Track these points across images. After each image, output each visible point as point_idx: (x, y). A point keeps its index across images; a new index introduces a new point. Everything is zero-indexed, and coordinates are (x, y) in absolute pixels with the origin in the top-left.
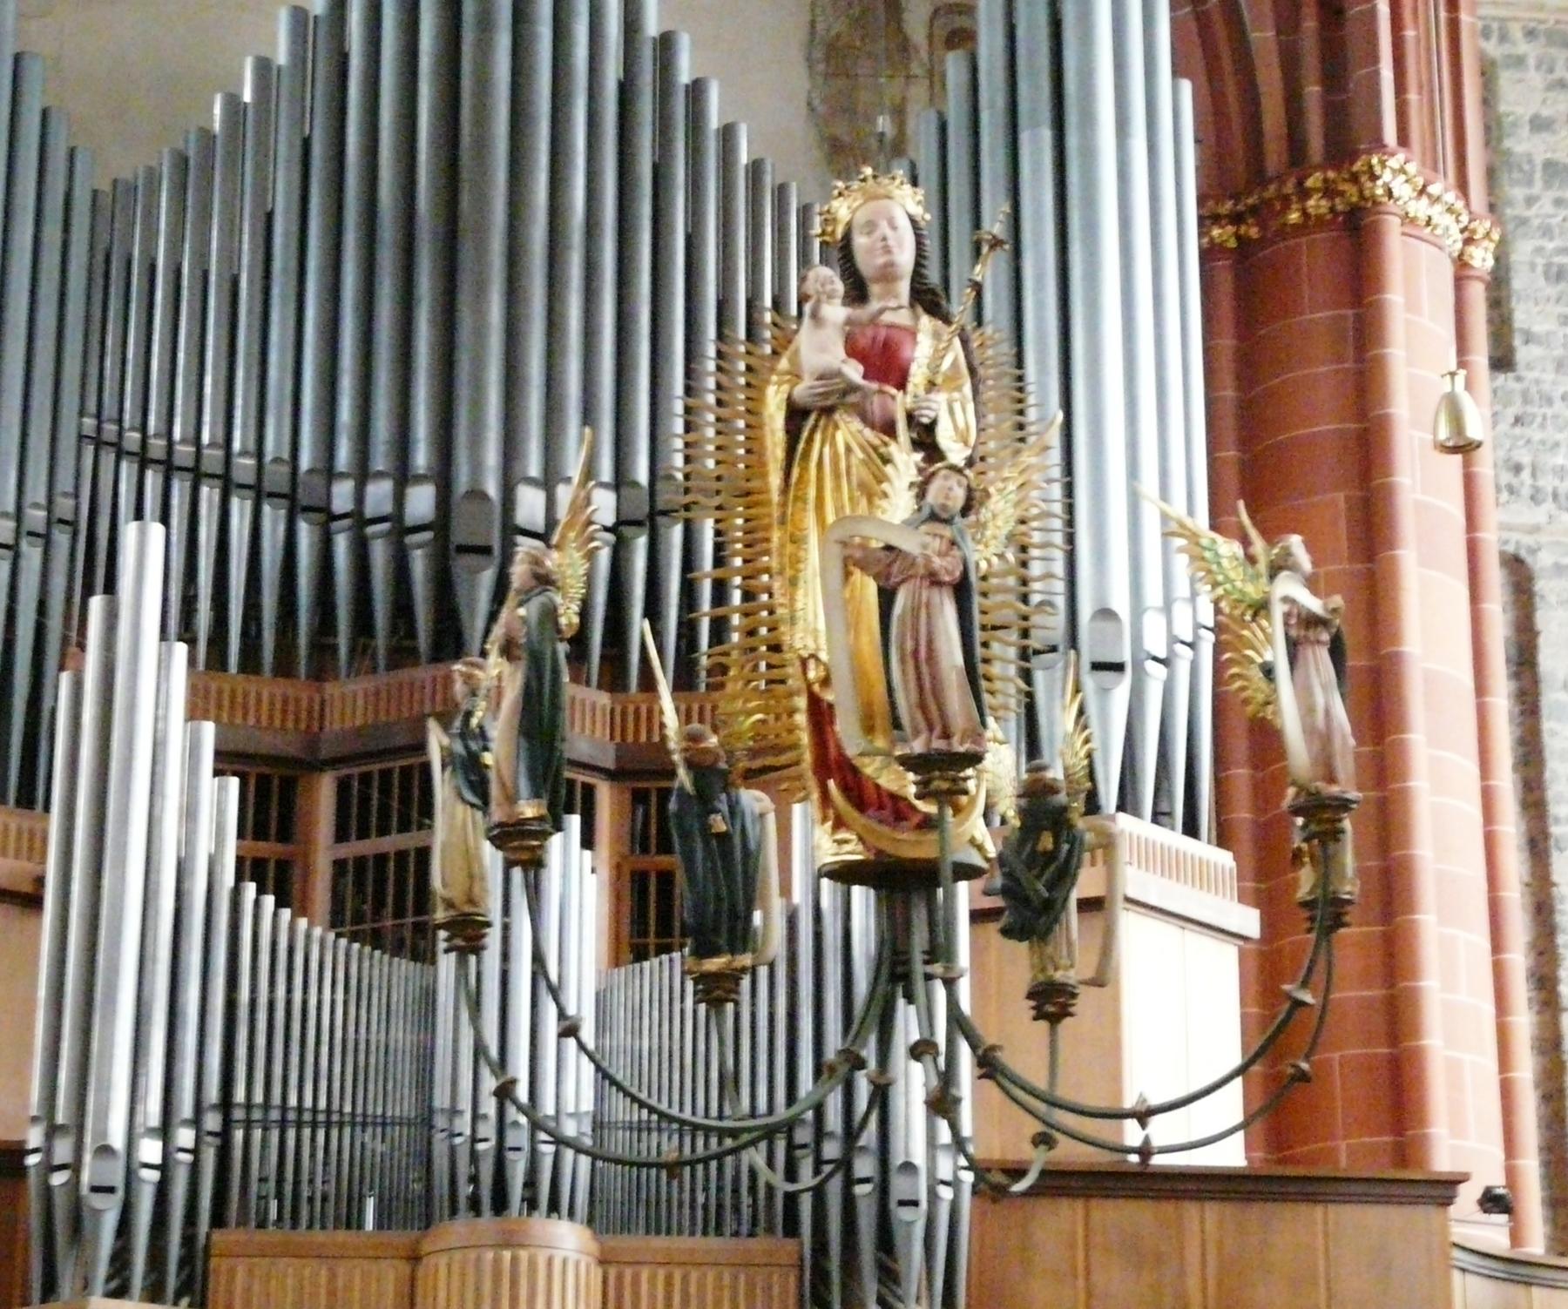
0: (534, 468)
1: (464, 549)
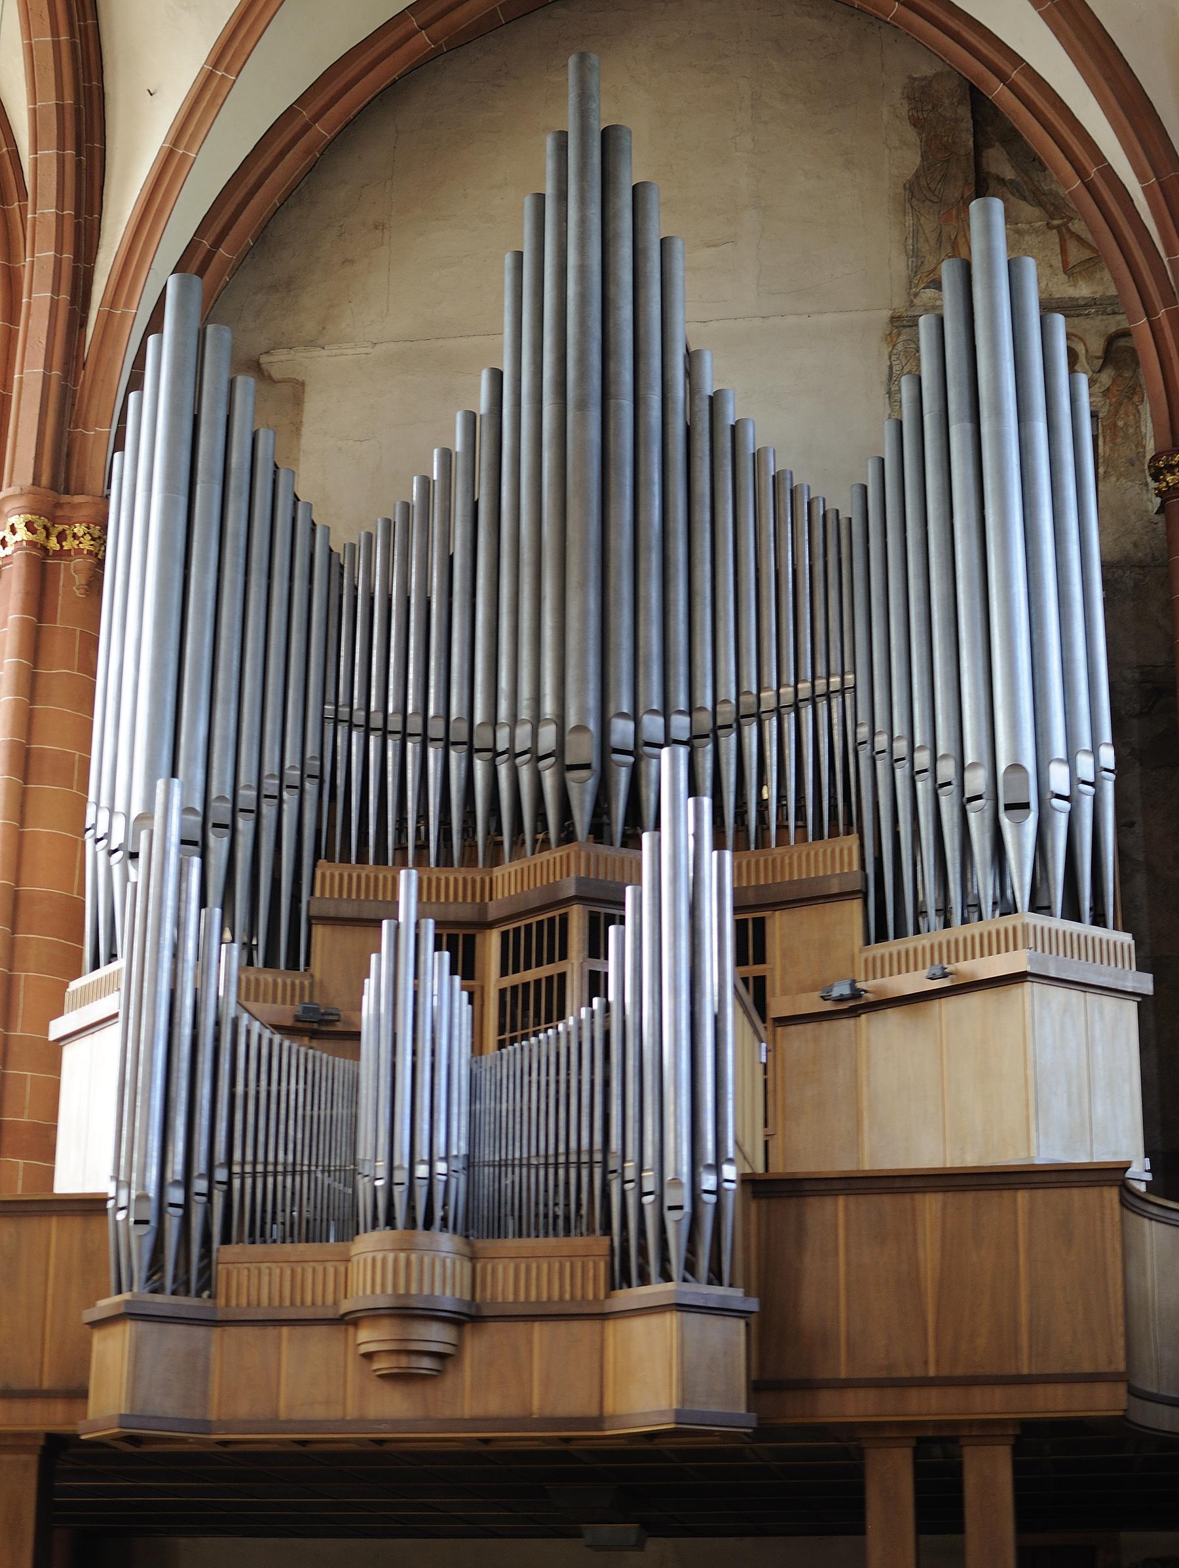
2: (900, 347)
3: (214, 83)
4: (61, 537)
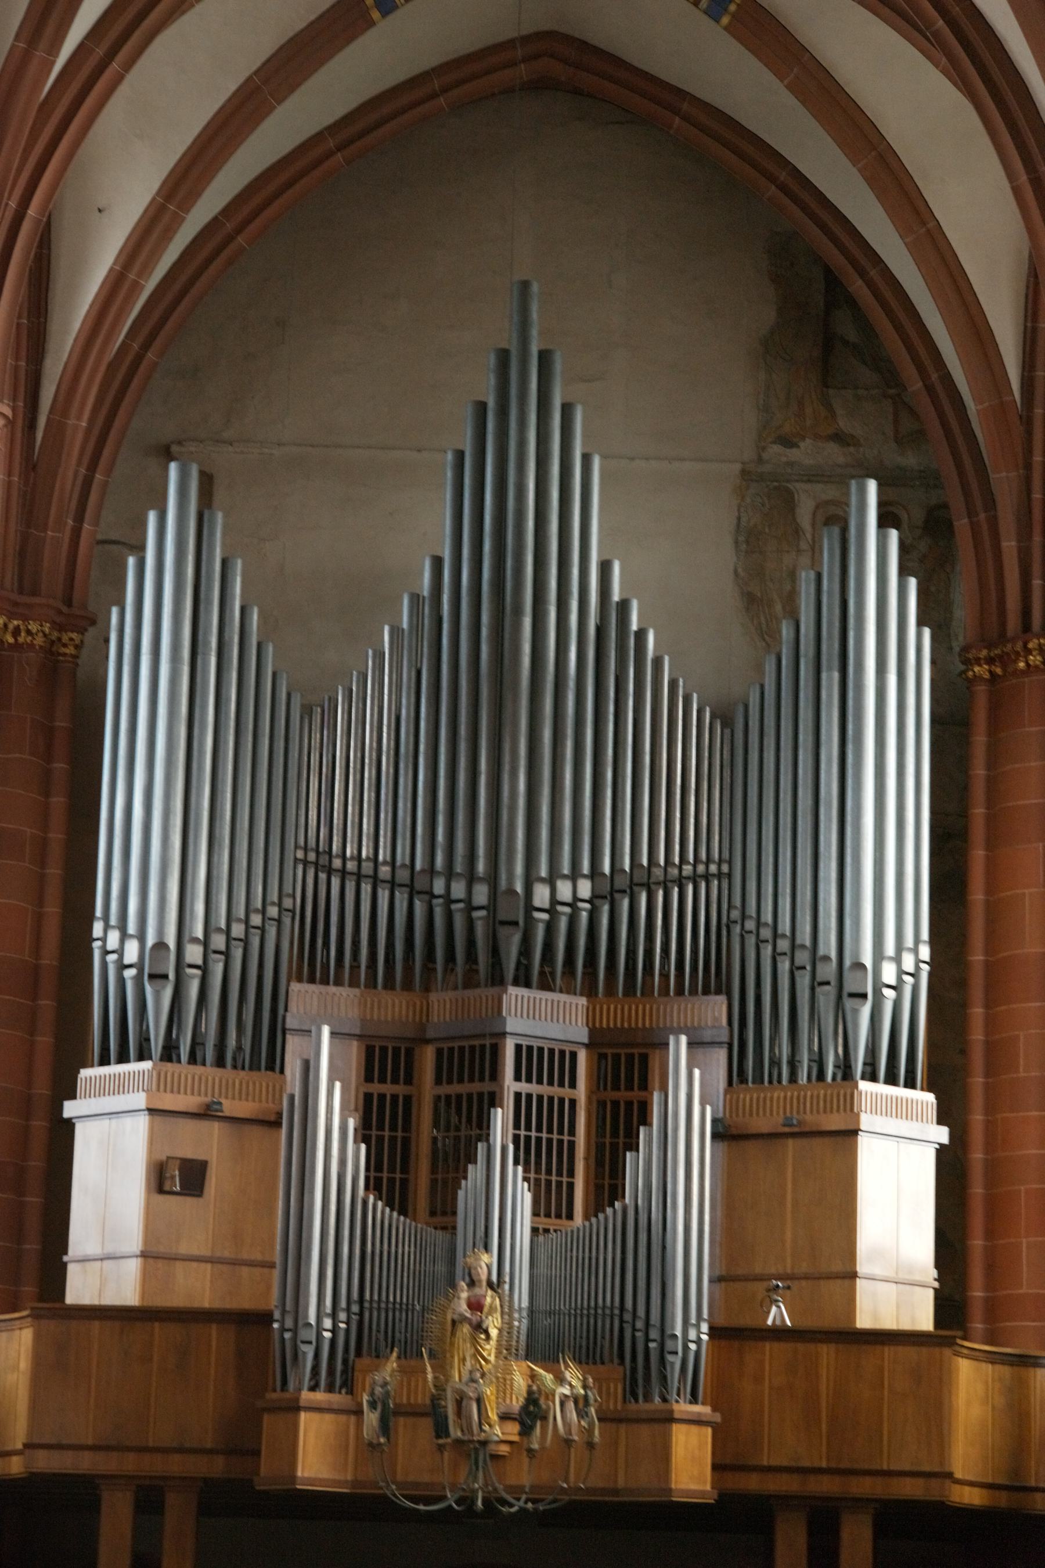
0: (544, 873)
1: (503, 923)
2: (748, 500)
3: (166, 219)
4: (16, 632)
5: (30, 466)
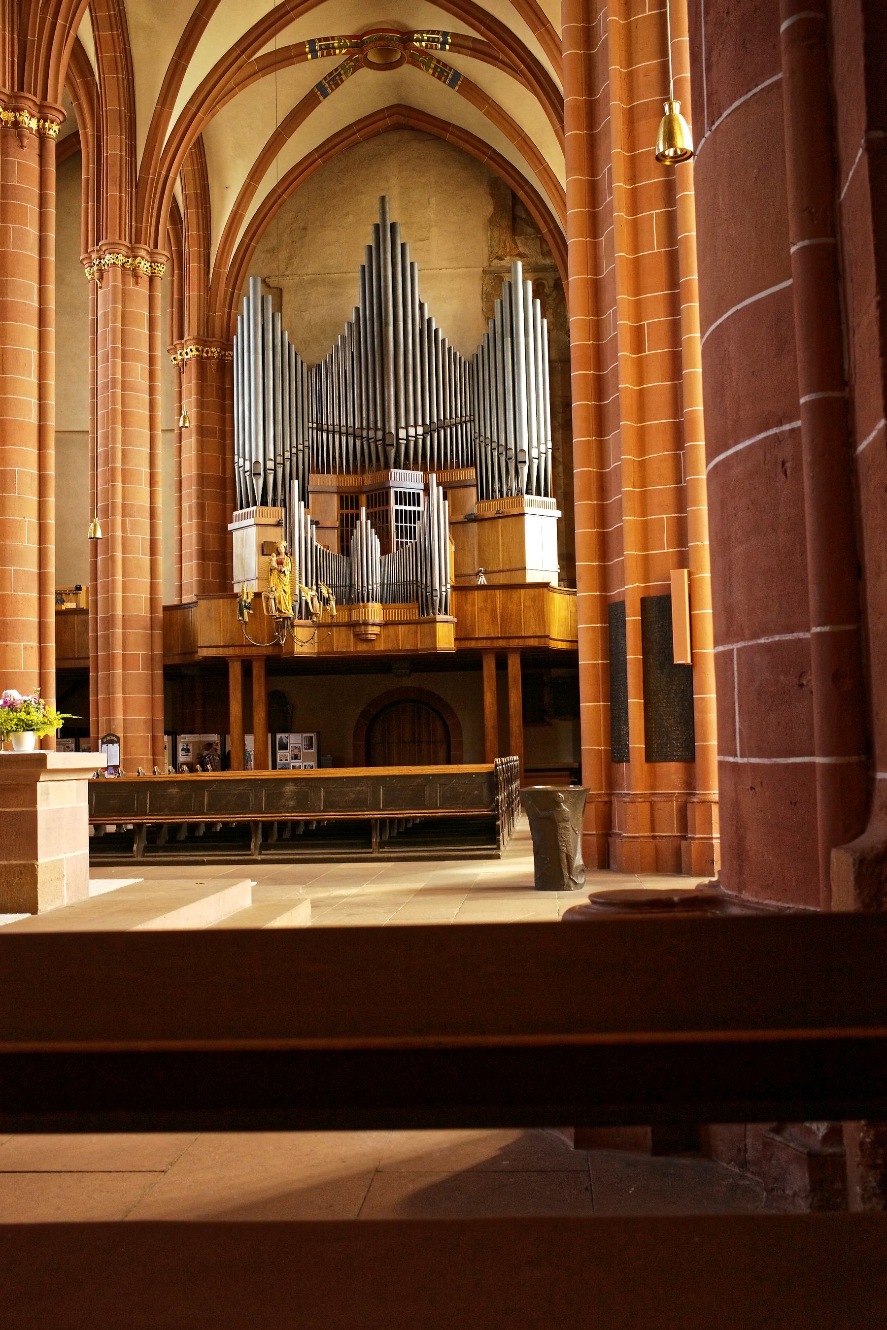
0: (403, 425)
4: (207, 352)
5: (208, 289)
